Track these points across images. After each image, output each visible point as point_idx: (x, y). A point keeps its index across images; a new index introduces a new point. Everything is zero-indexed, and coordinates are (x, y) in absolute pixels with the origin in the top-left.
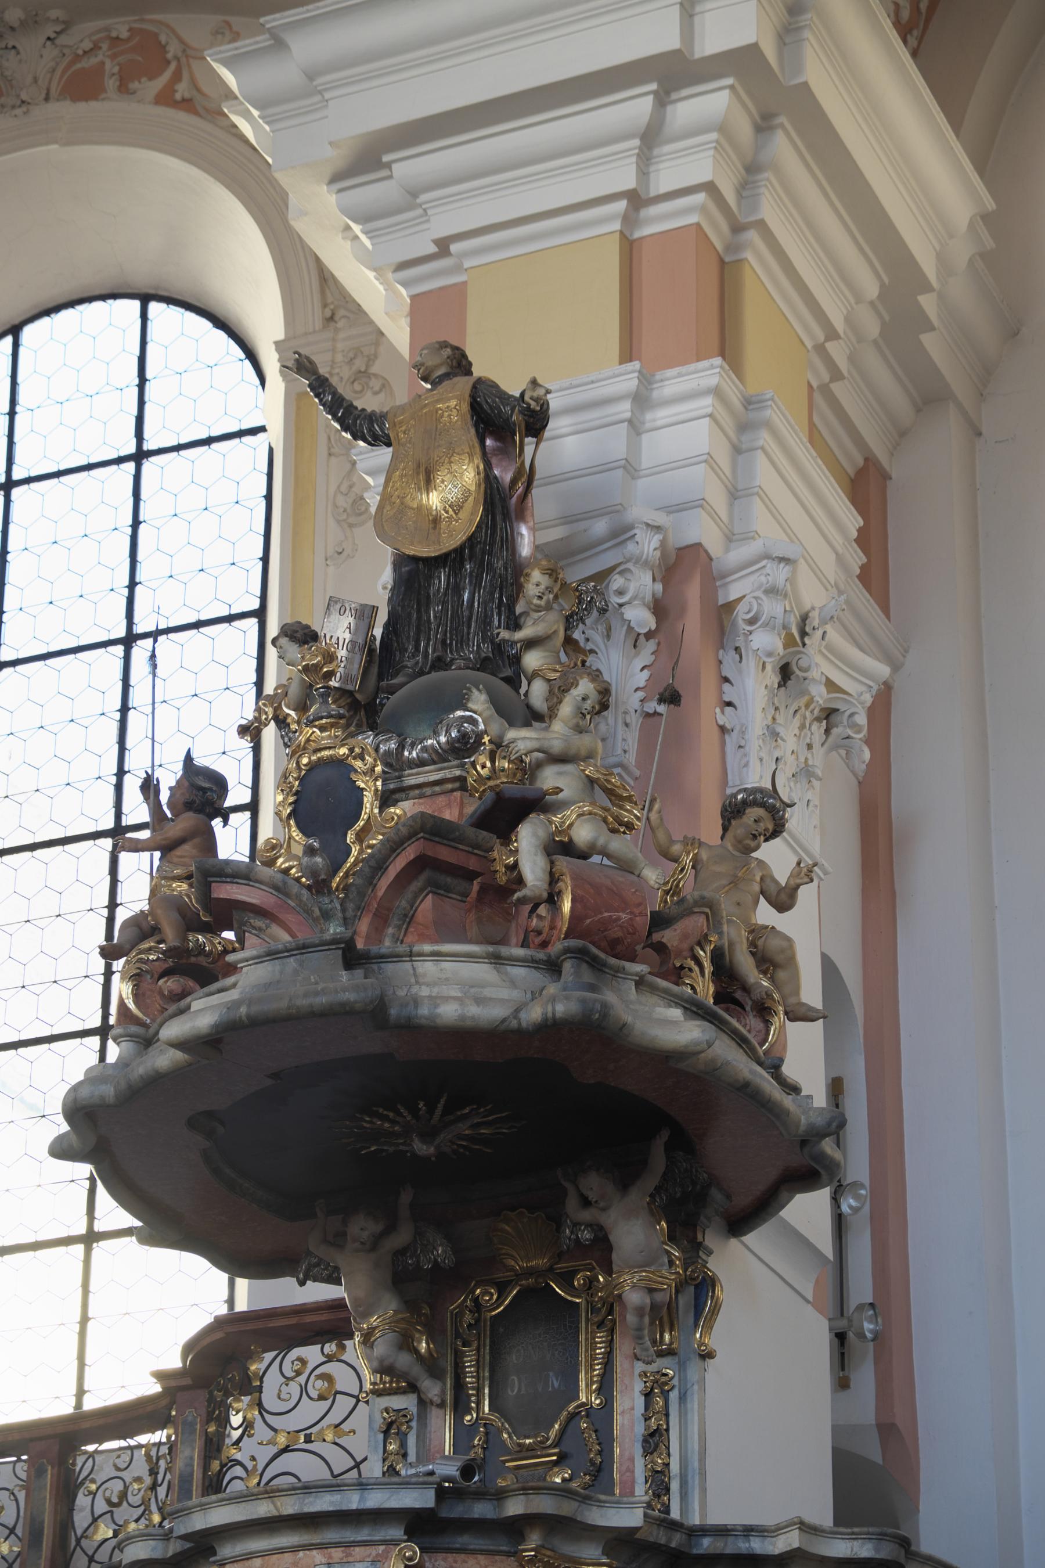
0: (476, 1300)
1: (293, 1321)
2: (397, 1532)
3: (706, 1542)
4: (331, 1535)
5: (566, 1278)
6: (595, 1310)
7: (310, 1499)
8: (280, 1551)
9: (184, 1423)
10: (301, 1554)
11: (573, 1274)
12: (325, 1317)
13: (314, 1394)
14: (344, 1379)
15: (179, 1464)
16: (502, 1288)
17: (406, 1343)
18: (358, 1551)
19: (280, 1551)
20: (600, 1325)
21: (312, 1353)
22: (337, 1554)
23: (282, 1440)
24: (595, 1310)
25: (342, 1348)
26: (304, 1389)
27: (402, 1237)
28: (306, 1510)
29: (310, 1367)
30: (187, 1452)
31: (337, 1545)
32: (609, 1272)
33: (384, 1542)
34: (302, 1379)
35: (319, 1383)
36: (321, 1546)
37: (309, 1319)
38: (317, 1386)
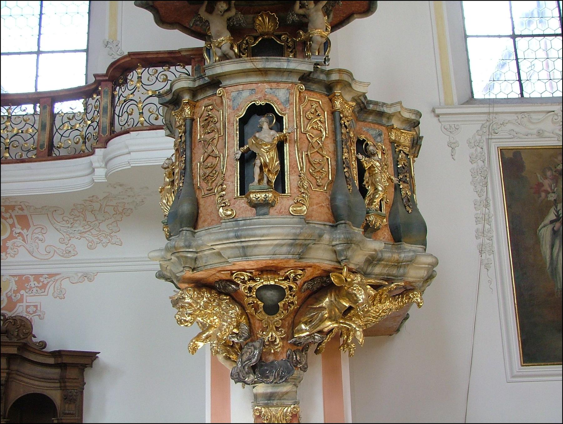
0: (247, 41)
1: (155, 56)
2: (295, 79)
3: (371, 106)
4: (271, 78)
5: (279, 37)
6: (289, 47)
7: (268, 63)
8: (251, 83)
9: (104, 91)
10: (259, 84)
11: (281, 35)
12: (166, 55)
13: (161, 80)
14: (171, 77)
15: (103, 104)
16: (256, 38)
17: (232, 48)
18: (282, 85)
19: (251, 83)
20: (291, 52)
21: (160, 69)
22: (274, 85)
23: (150, 93)
24: (289, 47)
25: (169, 68)
26: (157, 78)
27: (233, 12)
28: (267, 67)
29: (159, 72)
30: (106, 100)
31: (274, 82)
32: (306, 31)
33: (292, 83)
34: (156, 75)
35: (162, 77)
36: (269, 82)
37: (161, 56)
38: (161, 78)
